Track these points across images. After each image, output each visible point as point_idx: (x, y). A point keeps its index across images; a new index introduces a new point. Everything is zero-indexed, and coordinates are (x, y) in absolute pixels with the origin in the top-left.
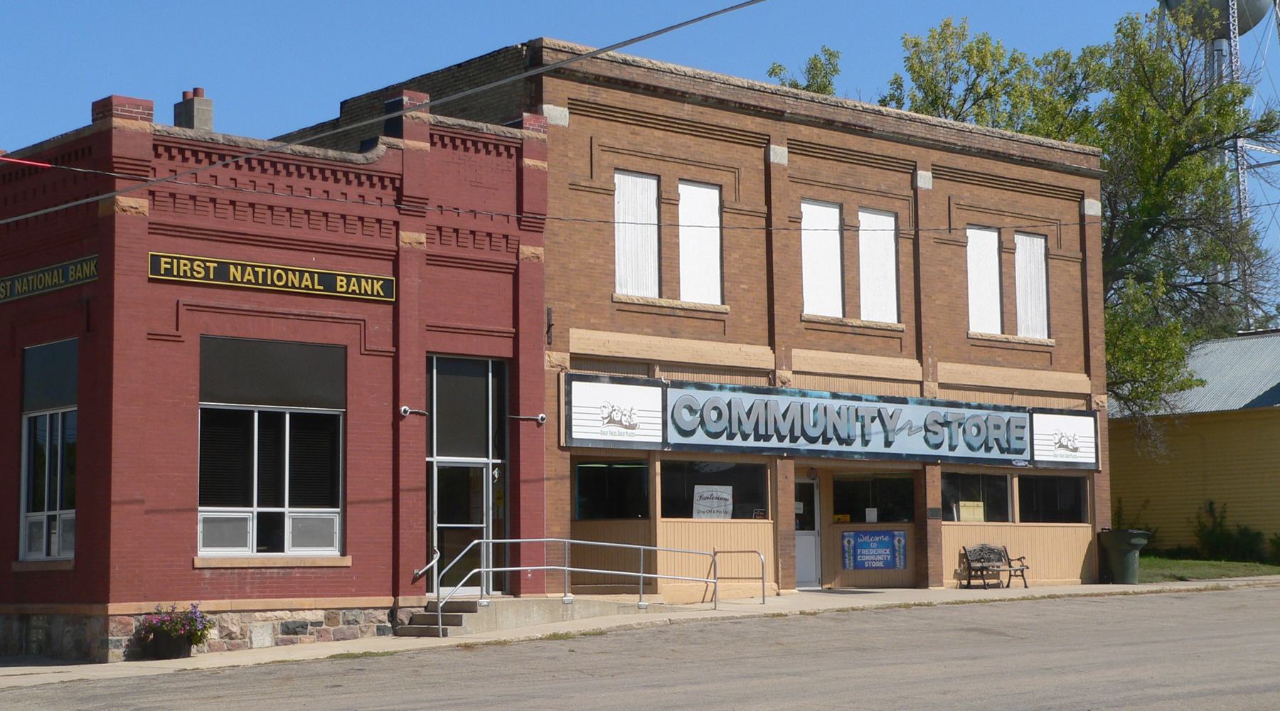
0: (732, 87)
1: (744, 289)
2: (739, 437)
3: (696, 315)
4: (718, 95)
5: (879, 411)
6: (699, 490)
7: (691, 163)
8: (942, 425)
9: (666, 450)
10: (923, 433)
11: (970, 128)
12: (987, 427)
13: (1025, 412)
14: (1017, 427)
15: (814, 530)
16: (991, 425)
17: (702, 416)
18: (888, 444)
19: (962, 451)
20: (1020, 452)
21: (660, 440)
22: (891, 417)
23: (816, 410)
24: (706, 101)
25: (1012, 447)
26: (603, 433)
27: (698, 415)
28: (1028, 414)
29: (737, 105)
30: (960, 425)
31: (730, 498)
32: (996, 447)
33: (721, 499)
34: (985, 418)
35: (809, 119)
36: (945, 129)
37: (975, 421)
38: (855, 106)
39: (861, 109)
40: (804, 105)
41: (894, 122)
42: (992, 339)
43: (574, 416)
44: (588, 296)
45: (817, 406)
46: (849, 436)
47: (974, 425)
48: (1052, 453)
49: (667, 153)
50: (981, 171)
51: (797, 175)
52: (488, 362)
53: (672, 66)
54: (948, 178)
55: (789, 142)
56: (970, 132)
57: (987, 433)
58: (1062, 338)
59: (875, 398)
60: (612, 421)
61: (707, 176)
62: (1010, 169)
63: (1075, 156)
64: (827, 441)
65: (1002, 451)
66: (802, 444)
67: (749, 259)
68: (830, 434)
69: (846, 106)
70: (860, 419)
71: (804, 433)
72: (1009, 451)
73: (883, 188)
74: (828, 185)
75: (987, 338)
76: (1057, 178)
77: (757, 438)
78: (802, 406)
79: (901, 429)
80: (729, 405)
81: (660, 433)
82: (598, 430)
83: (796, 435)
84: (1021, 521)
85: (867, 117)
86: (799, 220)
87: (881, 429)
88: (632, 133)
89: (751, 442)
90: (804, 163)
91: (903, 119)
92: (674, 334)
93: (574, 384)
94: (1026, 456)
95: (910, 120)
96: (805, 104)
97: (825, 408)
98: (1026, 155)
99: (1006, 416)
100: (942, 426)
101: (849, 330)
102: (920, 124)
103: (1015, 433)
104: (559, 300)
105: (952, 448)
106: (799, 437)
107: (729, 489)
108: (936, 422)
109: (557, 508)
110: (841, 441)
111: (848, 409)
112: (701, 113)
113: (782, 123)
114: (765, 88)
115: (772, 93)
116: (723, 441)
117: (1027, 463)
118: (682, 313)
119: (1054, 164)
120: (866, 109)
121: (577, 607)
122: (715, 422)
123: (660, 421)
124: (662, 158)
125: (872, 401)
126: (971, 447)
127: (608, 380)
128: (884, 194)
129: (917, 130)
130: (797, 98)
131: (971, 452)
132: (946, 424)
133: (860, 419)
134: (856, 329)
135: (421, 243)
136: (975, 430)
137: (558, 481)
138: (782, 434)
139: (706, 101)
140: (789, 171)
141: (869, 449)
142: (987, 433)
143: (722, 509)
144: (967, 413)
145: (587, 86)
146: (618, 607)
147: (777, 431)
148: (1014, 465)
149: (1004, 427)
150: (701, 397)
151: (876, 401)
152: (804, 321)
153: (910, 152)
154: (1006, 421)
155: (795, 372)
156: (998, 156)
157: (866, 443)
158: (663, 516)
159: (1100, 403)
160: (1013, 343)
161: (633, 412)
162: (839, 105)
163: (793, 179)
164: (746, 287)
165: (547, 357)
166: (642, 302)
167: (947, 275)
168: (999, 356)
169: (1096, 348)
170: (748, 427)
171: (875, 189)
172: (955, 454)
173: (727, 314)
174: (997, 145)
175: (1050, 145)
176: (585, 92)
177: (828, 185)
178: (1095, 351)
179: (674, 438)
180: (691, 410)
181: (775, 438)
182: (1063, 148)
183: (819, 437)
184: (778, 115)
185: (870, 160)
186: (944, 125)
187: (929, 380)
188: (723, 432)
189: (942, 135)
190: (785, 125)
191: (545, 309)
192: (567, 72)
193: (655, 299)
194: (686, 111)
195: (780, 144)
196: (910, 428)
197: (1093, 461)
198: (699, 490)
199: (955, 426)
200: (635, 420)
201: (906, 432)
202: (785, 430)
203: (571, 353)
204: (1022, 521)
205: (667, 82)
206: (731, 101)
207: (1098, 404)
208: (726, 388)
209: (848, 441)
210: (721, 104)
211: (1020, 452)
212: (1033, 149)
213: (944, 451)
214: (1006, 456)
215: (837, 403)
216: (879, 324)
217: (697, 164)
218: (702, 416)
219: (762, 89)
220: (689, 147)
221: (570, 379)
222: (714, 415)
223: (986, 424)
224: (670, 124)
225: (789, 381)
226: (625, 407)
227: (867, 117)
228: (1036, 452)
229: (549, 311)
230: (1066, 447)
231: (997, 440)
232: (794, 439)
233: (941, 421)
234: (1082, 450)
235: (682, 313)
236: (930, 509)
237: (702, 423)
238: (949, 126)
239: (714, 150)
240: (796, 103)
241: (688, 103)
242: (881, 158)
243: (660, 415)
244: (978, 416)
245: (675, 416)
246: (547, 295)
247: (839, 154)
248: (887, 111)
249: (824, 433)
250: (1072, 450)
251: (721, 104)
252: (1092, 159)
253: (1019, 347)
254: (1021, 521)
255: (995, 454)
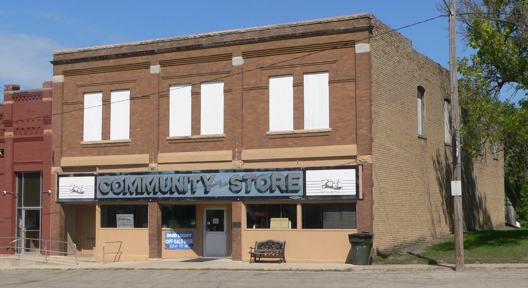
0: (132, 46)
1: (139, 131)
2: (128, 194)
3: (115, 145)
4: (126, 51)
5: (202, 178)
6: (118, 216)
7: (115, 83)
8: (241, 181)
9: (96, 201)
10: (229, 186)
11: (267, 28)
12: (271, 180)
13: (300, 170)
14: (293, 179)
15: (224, 231)
16: (274, 179)
17: (111, 187)
18: (206, 192)
19: (254, 193)
20: (296, 191)
21: (94, 197)
22: (208, 180)
23: (166, 179)
24: (117, 56)
25: (289, 189)
26: (70, 196)
27: (110, 186)
28: (302, 171)
29: (132, 54)
30: (252, 180)
31: (132, 219)
32: (277, 190)
33: (128, 220)
34: (270, 176)
35: (168, 50)
36: (251, 32)
37: (263, 178)
38: (195, 37)
39: (199, 37)
40: (168, 44)
41: (219, 38)
42: (283, 133)
43: (60, 190)
44: (71, 144)
45: (167, 178)
46: (184, 190)
47: (262, 180)
48: (320, 191)
49: (104, 81)
50: (276, 47)
51: (165, 76)
52: (40, 173)
53: (104, 46)
54: (256, 56)
55: (160, 62)
56: (268, 29)
57: (271, 183)
58: (338, 126)
59: (200, 172)
60: (74, 191)
61: (123, 86)
62: (296, 42)
63: (348, 22)
64: (172, 193)
65: (282, 192)
66: (159, 195)
67: (141, 117)
68: (174, 189)
69: (190, 38)
70: (190, 182)
71: (160, 190)
72: (287, 191)
73: (214, 70)
74: (183, 77)
75: (279, 134)
76: (333, 38)
77: (137, 194)
78: (159, 179)
79: (215, 185)
80: (124, 181)
81: (94, 194)
82: (69, 195)
83: (156, 191)
84: (303, 227)
85: (203, 40)
86: (192, 94)
87: (202, 185)
88: (91, 77)
89: (134, 196)
90: (170, 70)
91: (224, 35)
92: (106, 154)
93: (60, 178)
94: (301, 193)
95: (228, 34)
96: (168, 43)
97: (171, 179)
98: (308, 31)
99: (285, 173)
100: (241, 182)
101: (193, 141)
102: (235, 34)
103: (291, 181)
104: (56, 148)
105: (247, 192)
106: (158, 192)
107: (132, 215)
108: (237, 180)
109: (55, 225)
110: (179, 193)
111: (184, 178)
112: (117, 61)
113: (156, 55)
114: (147, 43)
115: (151, 43)
116: (121, 196)
117: (301, 197)
118: (109, 145)
119: (326, 32)
120: (201, 36)
121: (21, 261)
122: (117, 188)
123: (94, 190)
124: (103, 84)
125: (198, 173)
126: (260, 191)
127: (73, 175)
128: (215, 73)
129: (233, 38)
130: (165, 42)
131: (259, 193)
132: (245, 180)
133: (190, 182)
134: (197, 140)
135: (11, 135)
136: (263, 183)
137: (56, 214)
138: (149, 191)
139: (117, 56)
140: (162, 75)
141: (196, 195)
142: (271, 183)
143: (129, 224)
144: (257, 174)
145: (70, 65)
146: (36, 262)
147: (147, 190)
148: (291, 199)
149: (283, 180)
150: (112, 178)
151: (200, 173)
152: (167, 140)
153: (229, 49)
154: (285, 176)
155: (159, 164)
156: (285, 37)
157: (193, 192)
158: (103, 225)
159: (362, 160)
160: (299, 133)
161: (83, 187)
162: (186, 38)
163: (164, 78)
164: (139, 130)
165: (52, 170)
166: (92, 143)
167: (254, 105)
168: (290, 142)
169: (361, 129)
170: (133, 189)
171: (209, 72)
172: (250, 195)
173: (130, 142)
174: (287, 32)
175: (326, 21)
176: (69, 67)
177: (183, 77)
178: (361, 130)
179: (99, 196)
180: (107, 184)
181: (146, 193)
182: (337, 20)
183: (168, 191)
184: (152, 53)
185: (206, 59)
186: (249, 31)
187: (236, 159)
188: (121, 192)
189: (249, 36)
190: (158, 56)
191: (52, 151)
192: (60, 62)
193: (100, 141)
194: (111, 62)
195: (156, 64)
196: (221, 184)
197: (355, 194)
198: (118, 216)
199: (249, 181)
200: (83, 190)
201: (218, 186)
202: (150, 189)
203: (62, 167)
204: (304, 227)
205: (103, 53)
206: (128, 53)
207: (360, 161)
208: (123, 174)
209: (184, 192)
210: (125, 55)
211: (296, 191)
212: (314, 26)
213: (242, 194)
214: (285, 194)
215: (178, 176)
216: (208, 136)
217: (118, 82)
218: (111, 187)
219: (146, 43)
220: (115, 76)
221: (59, 176)
222: (117, 185)
223: (270, 179)
224: (105, 69)
225: (154, 168)
226: (79, 185)
227: (203, 40)
228: (307, 191)
229: (53, 152)
230: (332, 187)
231: (278, 187)
232: (155, 193)
233: (241, 179)
234: (344, 188)
235: (109, 145)
236: (234, 223)
237: (112, 189)
238: (253, 30)
239: (127, 75)
240: (164, 44)
241: (112, 59)
242: (211, 57)
243: (94, 187)
244: (265, 175)
245: (100, 187)
246: (53, 146)
247: (189, 61)
248: (213, 34)
249: (171, 190)
250: (336, 189)
251: (125, 55)
252: (361, 21)
253: (303, 135)
254: (303, 227)
255: (277, 193)
